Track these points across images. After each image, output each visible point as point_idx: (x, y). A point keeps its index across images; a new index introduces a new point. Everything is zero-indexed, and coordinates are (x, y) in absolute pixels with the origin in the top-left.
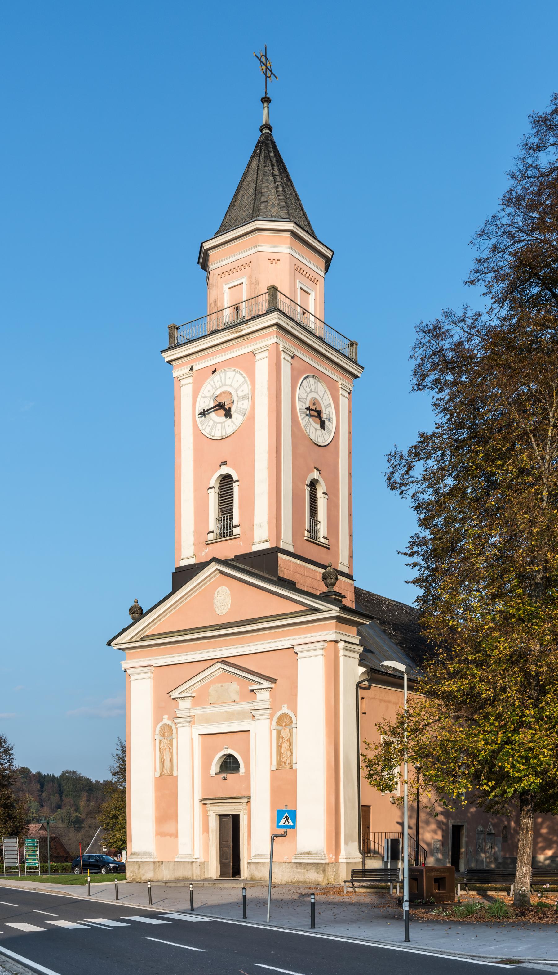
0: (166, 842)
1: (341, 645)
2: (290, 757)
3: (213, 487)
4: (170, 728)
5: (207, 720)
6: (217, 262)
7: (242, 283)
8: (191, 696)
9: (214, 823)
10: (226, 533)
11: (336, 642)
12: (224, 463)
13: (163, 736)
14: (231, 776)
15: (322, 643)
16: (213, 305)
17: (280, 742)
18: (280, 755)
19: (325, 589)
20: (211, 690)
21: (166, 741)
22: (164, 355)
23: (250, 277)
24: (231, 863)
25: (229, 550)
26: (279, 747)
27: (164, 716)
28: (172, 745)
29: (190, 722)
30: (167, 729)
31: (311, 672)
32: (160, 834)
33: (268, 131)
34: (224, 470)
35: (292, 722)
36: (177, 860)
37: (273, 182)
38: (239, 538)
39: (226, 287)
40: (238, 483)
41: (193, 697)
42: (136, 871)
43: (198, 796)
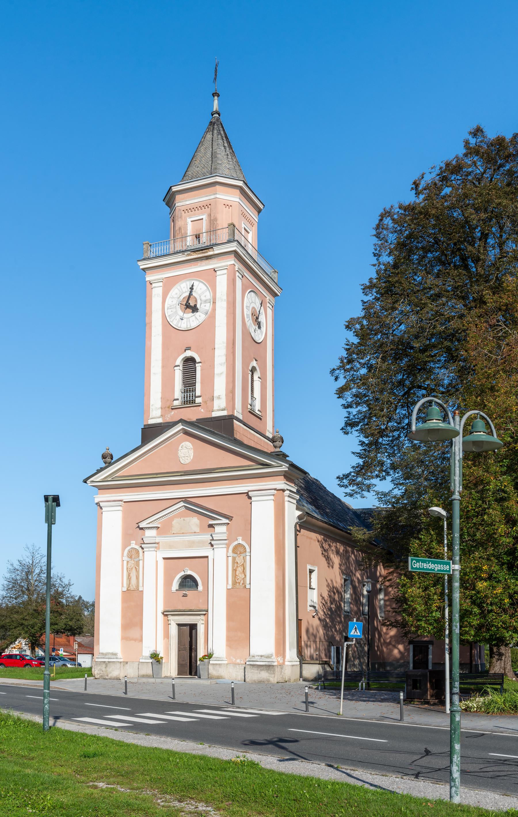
0: (126, 646)
1: (287, 492)
2: (244, 579)
3: (179, 366)
4: (138, 552)
5: (171, 547)
6: (182, 202)
7: (202, 219)
8: (156, 527)
9: (174, 630)
10: (189, 401)
11: (283, 490)
12: (189, 348)
13: (131, 557)
14: (190, 593)
15: (273, 491)
16: (178, 232)
19: (273, 450)
20: (175, 522)
21: (133, 562)
22: (140, 263)
23: (210, 215)
24: (190, 664)
25: (192, 414)
26: (234, 570)
27: (132, 542)
28: (138, 566)
29: (156, 547)
30: (134, 552)
31: (263, 513)
32: (125, 638)
33: (217, 116)
34: (189, 354)
35: (246, 551)
36: (141, 661)
37: (224, 151)
38: (200, 406)
39: (189, 220)
40: (200, 364)
41: (159, 528)
42: (104, 669)
43: (161, 608)
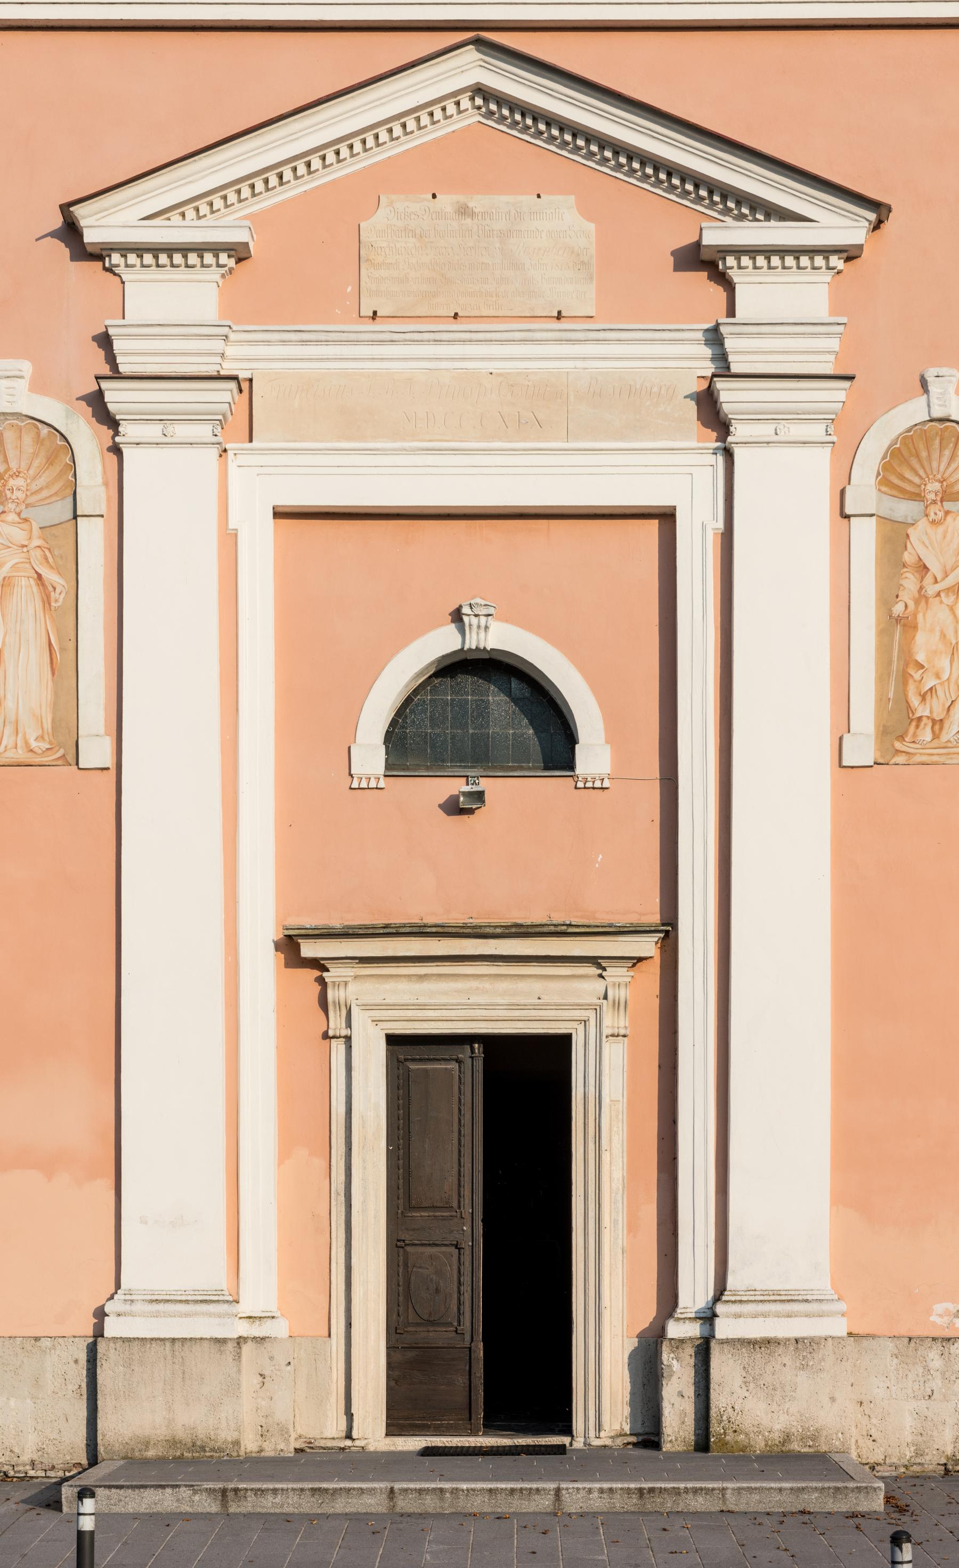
17: (906, 596)
18: (904, 678)
26: (897, 626)
